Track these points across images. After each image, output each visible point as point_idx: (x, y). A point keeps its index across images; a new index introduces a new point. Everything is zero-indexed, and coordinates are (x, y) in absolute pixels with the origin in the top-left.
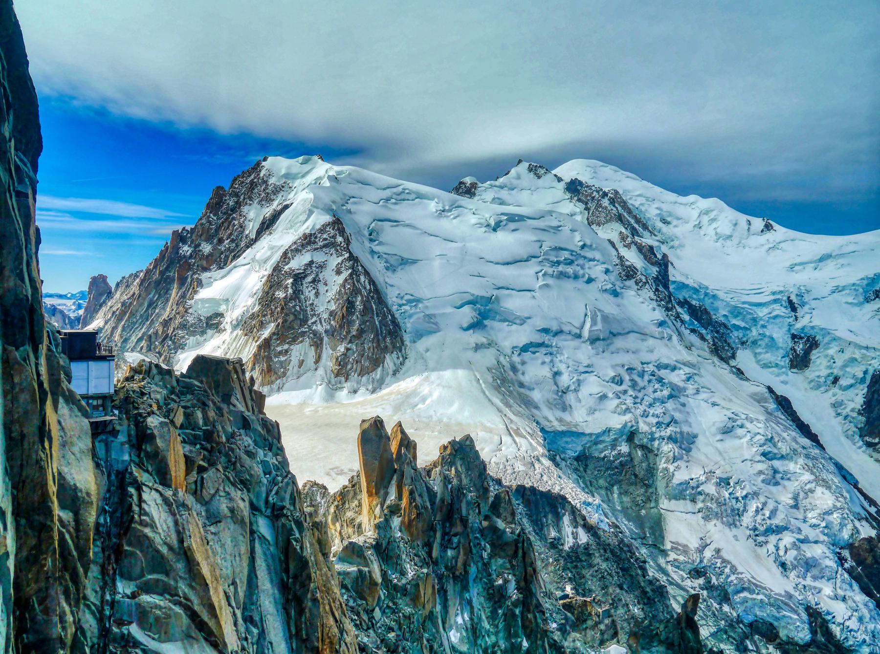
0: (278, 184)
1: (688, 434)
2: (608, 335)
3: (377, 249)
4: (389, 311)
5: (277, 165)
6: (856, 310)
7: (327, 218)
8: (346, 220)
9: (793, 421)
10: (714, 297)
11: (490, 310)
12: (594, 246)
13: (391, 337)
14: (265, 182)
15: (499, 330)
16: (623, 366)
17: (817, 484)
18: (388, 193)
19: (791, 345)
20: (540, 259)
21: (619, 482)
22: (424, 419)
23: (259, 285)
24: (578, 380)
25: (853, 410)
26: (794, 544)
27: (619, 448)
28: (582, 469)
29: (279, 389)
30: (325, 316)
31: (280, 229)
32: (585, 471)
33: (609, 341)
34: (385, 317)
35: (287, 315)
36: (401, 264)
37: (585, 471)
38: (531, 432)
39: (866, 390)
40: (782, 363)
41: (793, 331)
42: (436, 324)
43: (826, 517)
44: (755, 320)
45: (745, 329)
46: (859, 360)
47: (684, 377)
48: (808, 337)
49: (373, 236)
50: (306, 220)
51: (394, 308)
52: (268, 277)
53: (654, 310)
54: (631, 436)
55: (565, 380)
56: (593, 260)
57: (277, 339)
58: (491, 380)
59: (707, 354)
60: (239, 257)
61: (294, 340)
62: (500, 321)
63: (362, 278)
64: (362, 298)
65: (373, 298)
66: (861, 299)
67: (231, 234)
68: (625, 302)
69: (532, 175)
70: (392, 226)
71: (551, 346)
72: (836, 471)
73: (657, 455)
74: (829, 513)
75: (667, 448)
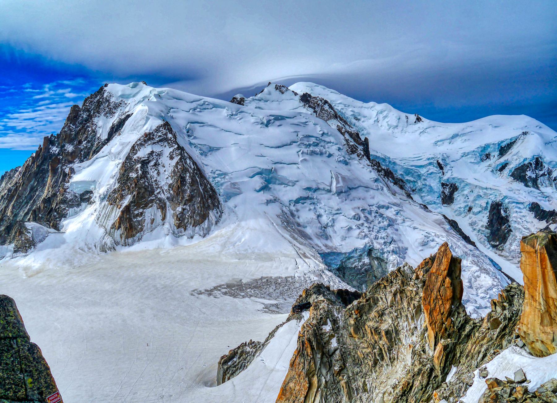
0: (117, 102)
1: (402, 248)
2: (347, 190)
3: (193, 141)
4: (208, 181)
5: (115, 89)
6: (476, 166)
7: (160, 122)
8: (171, 122)
9: (460, 235)
10: (394, 163)
11: (272, 178)
12: (329, 134)
13: (211, 199)
14: (108, 101)
15: (279, 190)
16: (359, 208)
17: (481, 272)
18: (194, 105)
19: (442, 190)
20: (298, 143)
21: (366, 282)
22: (243, 252)
23: (117, 170)
24: (333, 219)
25: (482, 226)
26: (474, 310)
27: (363, 261)
28: (342, 276)
29: (139, 240)
30: (166, 188)
31: (126, 131)
32: (344, 277)
33: (348, 193)
34: (206, 186)
35: (140, 188)
36: (210, 151)
37: (344, 277)
38: (313, 254)
39: (488, 214)
40: (438, 201)
41: (442, 181)
42: (239, 189)
43: (489, 292)
44: (419, 176)
45: (415, 182)
46: (483, 196)
47: (395, 213)
48: (451, 184)
49: (189, 133)
50: (145, 124)
51: (211, 180)
52: (123, 164)
53: (371, 172)
54: (370, 252)
55: (325, 219)
56: (330, 142)
57: (134, 206)
58: (280, 223)
59: (405, 198)
60: (98, 151)
61: (146, 206)
62: (279, 184)
63: (188, 161)
64: (190, 174)
65: (196, 174)
66: (479, 159)
67: (87, 137)
68: (352, 168)
69: (278, 91)
70: (200, 126)
71: (313, 199)
72: (491, 263)
73: (386, 263)
74: (490, 289)
75: (392, 258)
